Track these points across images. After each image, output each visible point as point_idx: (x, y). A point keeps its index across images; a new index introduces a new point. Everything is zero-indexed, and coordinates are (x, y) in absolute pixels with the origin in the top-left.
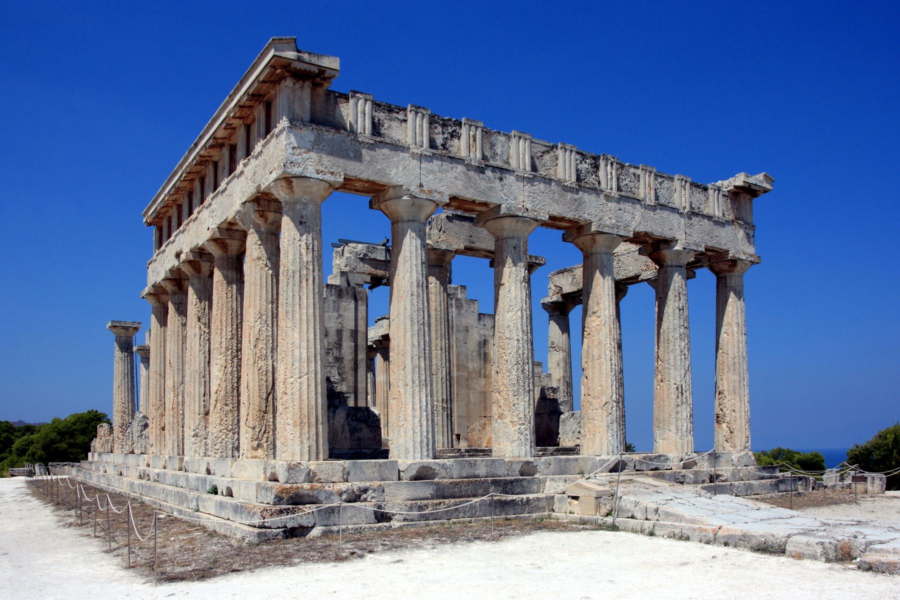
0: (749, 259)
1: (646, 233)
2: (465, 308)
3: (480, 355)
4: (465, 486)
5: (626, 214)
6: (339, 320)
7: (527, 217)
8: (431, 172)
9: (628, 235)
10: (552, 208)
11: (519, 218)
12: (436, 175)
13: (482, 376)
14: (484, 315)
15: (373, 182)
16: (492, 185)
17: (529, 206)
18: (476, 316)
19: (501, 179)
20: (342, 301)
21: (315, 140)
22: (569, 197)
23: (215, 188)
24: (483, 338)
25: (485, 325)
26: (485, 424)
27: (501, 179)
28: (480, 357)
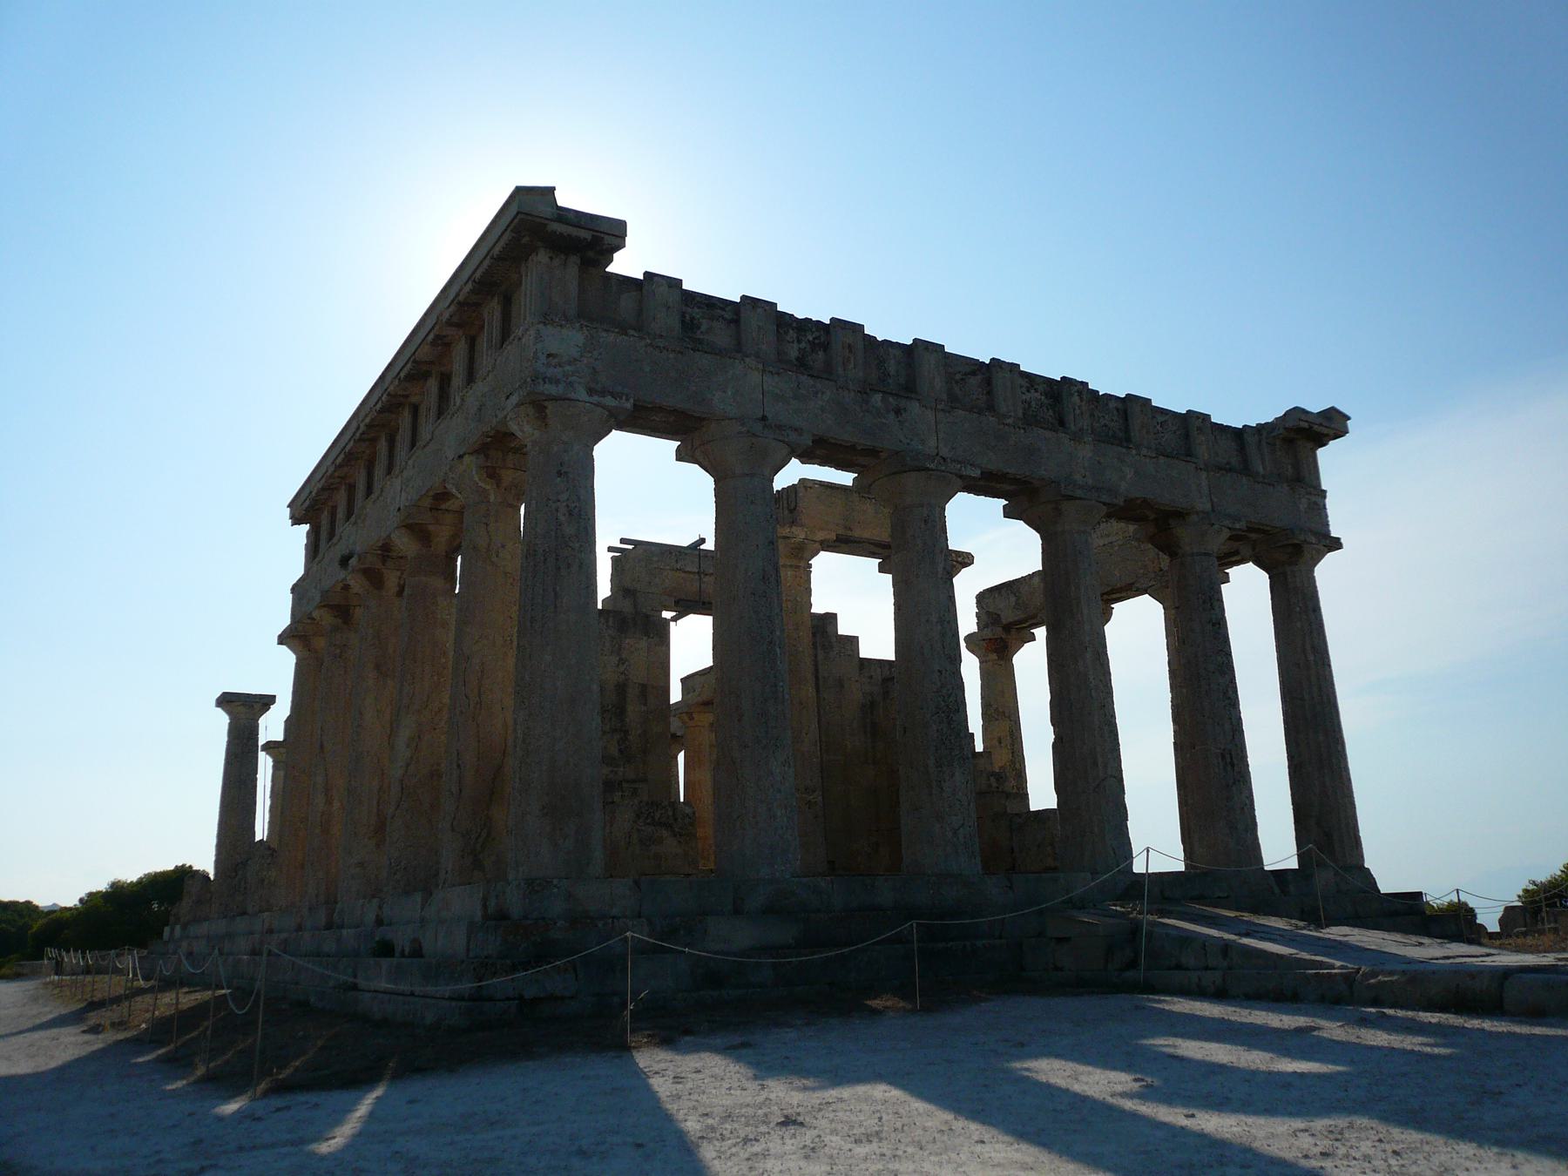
1: (1145, 501)
6: (622, 668)
7: (943, 471)
9: (1115, 501)
11: (931, 472)
15: (682, 412)
16: (884, 421)
17: (945, 452)
20: (626, 638)
21: (584, 344)
23: (413, 444)
25: (871, 677)
27: (898, 412)
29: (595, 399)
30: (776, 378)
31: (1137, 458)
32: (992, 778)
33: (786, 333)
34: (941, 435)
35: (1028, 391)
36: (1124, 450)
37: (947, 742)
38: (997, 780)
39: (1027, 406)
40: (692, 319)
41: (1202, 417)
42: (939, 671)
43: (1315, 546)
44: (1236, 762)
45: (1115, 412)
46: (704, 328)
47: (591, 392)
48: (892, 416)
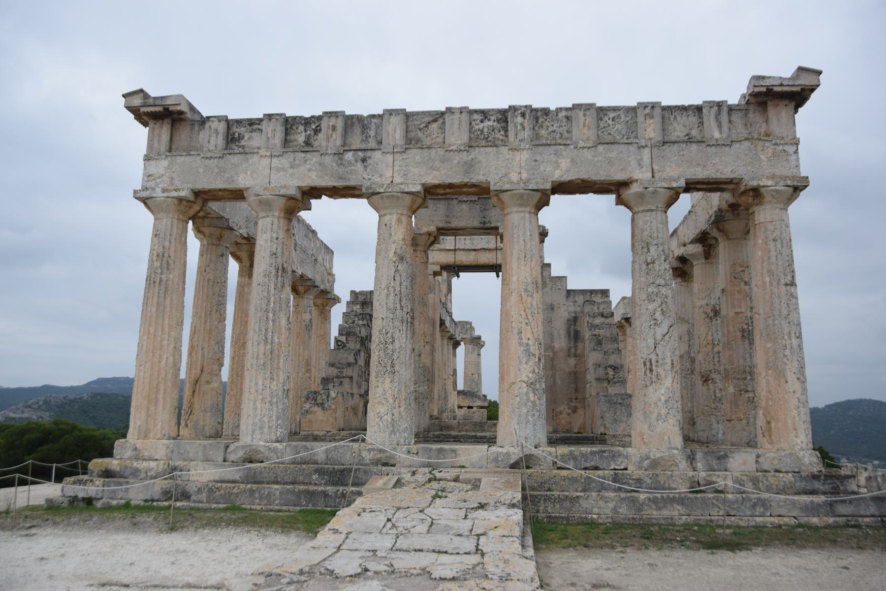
0: (782, 183)
2: (549, 286)
3: (569, 333)
4: (281, 472)
5: (545, 164)
8: (283, 169)
10: (431, 176)
12: (286, 171)
13: (572, 355)
14: (574, 291)
17: (398, 179)
18: (565, 293)
19: (364, 160)
21: (169, 165)
22: (456, 161)
24: (574, 315)
26: (576, 407)
27: (364, 160)
28: (569, 336)
29: (166, 194)
30: (280, 158)
31: (576, 150)
32: (609, 369)
33: (297, 128)
34: (395, 169)
35: (482, 121)
36: (562, 147)
37: (382, 362)
38: (614, 369)
39: (479, 133)
40: (239, 134)
41: (651, 105)
42: (383, 319)
43: (773, 188)
44: (654, 368)
45: (565, 120)
46: (246, 138)
47: (164, 191)
48: (359, 164)
